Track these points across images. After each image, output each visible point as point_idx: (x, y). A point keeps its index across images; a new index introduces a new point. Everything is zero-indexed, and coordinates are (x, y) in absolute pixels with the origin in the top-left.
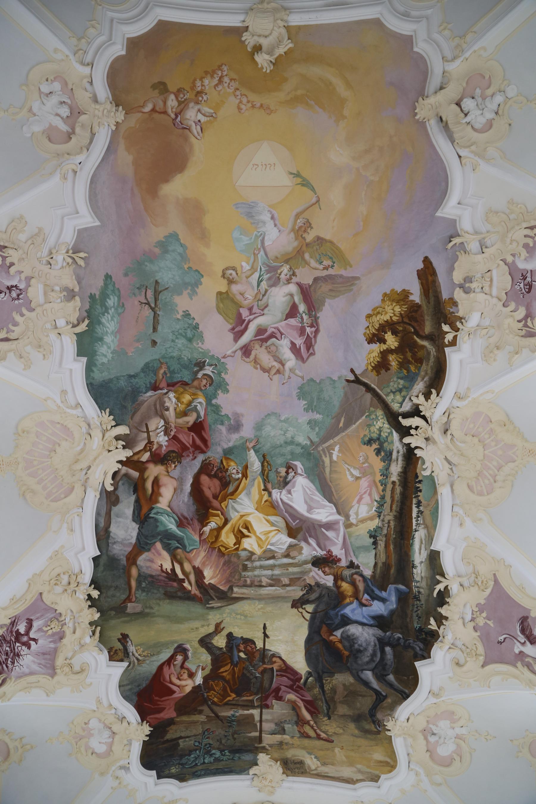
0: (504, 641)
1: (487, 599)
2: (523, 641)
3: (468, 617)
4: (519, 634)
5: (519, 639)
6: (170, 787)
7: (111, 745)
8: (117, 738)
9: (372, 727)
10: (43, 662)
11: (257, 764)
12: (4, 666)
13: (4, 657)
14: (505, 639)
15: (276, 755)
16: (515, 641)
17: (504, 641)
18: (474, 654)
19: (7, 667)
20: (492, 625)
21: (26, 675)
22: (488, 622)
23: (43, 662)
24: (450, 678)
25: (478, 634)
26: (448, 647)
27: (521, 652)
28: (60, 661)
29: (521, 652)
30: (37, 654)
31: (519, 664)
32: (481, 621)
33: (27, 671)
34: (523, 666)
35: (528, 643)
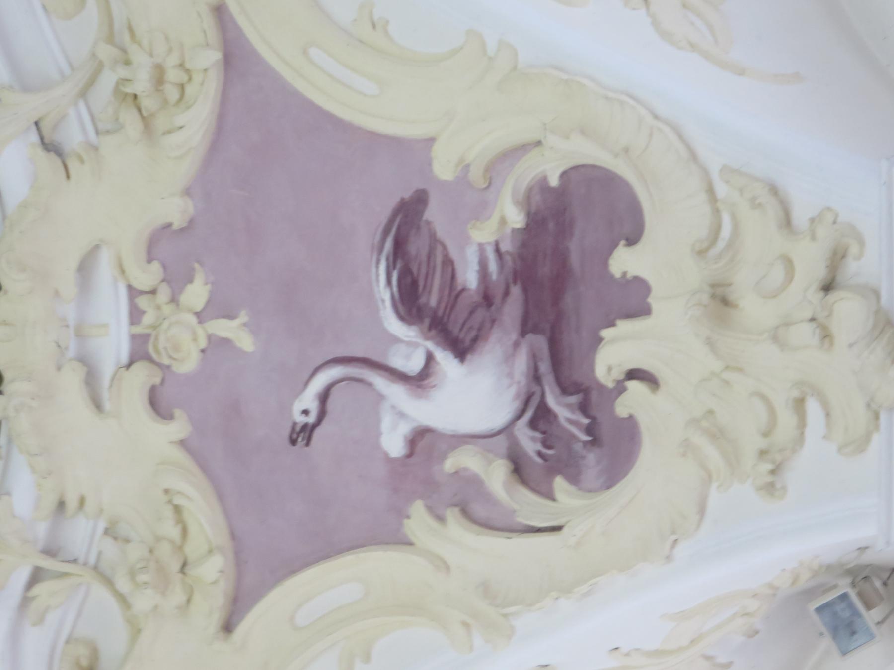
0: (322, 414)
1: (200, 187)
2: (414, 364)
3: (113, 346)
5: (397, 362)
14: (324, 397)
16: (379, 381)
17: (322, 414)
18: (175, 566)
20: (246, 342)
22: (223, 328)
25: (179, 428)
26: (23, 575)
27: (421, 438)
29: (421, 438)
31: (418, 521)
32: (184, 343)
34: (441, 519)
35: (445, 360)
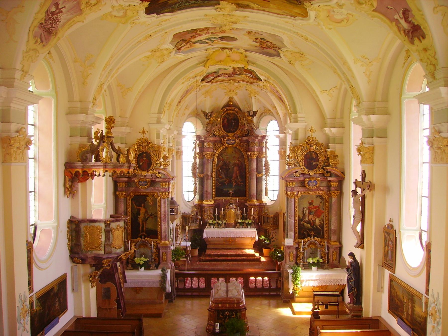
4: (401, 13)
6: (167, 17)
7: (126, 13)
8: (128, 11)
9: (296, 2)
10: (73, 12)
11: (219, 4)
12: (52, 28)
13: (50, 26)
14: (391, 9)
15: (232, 2)
19: (54, 27)
21: (66, 23)
23: (73, 12)
24: (351, 3)
28: (83, 7)
30: (68, 11)
33: (65, 21)
